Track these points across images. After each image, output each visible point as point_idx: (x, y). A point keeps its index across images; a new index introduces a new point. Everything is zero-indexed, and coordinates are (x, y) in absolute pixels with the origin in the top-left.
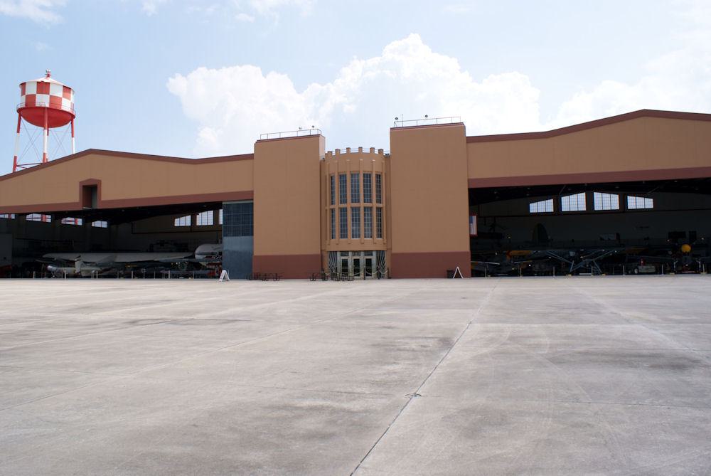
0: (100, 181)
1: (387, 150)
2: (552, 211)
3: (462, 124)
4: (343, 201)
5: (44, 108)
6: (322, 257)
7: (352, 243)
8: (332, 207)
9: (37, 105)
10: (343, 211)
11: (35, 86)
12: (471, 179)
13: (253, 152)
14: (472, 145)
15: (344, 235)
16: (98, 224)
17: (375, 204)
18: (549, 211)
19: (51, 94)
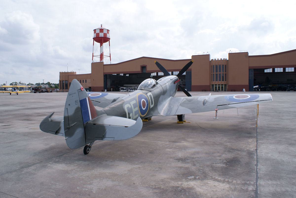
0: (147, 65)
1: (228, 59)
2: (272, 72)
3: (248, 52)
4: (217, 71)
5: (102, 37)
6: (210, 85)
7: (217, 83)
8: (213, 73)
9: (100, 36)
10: (217, 75)
11: (99, 30)
12: (250, 67)
13: (191, 58)
14: (250, 58)
15: (217, 80)
16: (127, 75)
17: (225, 73)
18: (271, 72)
19: (104, 32)
